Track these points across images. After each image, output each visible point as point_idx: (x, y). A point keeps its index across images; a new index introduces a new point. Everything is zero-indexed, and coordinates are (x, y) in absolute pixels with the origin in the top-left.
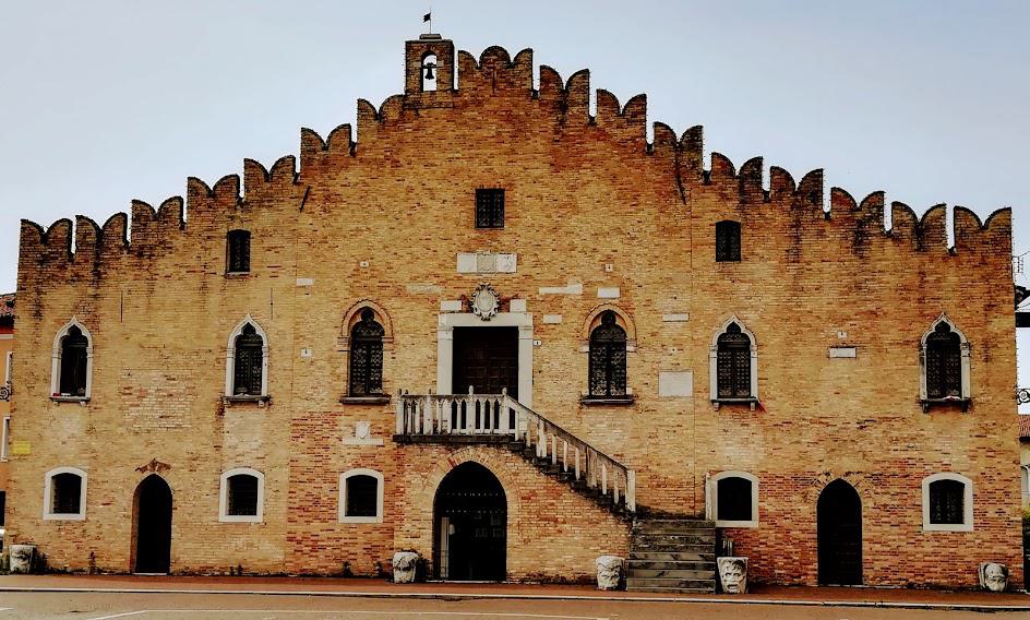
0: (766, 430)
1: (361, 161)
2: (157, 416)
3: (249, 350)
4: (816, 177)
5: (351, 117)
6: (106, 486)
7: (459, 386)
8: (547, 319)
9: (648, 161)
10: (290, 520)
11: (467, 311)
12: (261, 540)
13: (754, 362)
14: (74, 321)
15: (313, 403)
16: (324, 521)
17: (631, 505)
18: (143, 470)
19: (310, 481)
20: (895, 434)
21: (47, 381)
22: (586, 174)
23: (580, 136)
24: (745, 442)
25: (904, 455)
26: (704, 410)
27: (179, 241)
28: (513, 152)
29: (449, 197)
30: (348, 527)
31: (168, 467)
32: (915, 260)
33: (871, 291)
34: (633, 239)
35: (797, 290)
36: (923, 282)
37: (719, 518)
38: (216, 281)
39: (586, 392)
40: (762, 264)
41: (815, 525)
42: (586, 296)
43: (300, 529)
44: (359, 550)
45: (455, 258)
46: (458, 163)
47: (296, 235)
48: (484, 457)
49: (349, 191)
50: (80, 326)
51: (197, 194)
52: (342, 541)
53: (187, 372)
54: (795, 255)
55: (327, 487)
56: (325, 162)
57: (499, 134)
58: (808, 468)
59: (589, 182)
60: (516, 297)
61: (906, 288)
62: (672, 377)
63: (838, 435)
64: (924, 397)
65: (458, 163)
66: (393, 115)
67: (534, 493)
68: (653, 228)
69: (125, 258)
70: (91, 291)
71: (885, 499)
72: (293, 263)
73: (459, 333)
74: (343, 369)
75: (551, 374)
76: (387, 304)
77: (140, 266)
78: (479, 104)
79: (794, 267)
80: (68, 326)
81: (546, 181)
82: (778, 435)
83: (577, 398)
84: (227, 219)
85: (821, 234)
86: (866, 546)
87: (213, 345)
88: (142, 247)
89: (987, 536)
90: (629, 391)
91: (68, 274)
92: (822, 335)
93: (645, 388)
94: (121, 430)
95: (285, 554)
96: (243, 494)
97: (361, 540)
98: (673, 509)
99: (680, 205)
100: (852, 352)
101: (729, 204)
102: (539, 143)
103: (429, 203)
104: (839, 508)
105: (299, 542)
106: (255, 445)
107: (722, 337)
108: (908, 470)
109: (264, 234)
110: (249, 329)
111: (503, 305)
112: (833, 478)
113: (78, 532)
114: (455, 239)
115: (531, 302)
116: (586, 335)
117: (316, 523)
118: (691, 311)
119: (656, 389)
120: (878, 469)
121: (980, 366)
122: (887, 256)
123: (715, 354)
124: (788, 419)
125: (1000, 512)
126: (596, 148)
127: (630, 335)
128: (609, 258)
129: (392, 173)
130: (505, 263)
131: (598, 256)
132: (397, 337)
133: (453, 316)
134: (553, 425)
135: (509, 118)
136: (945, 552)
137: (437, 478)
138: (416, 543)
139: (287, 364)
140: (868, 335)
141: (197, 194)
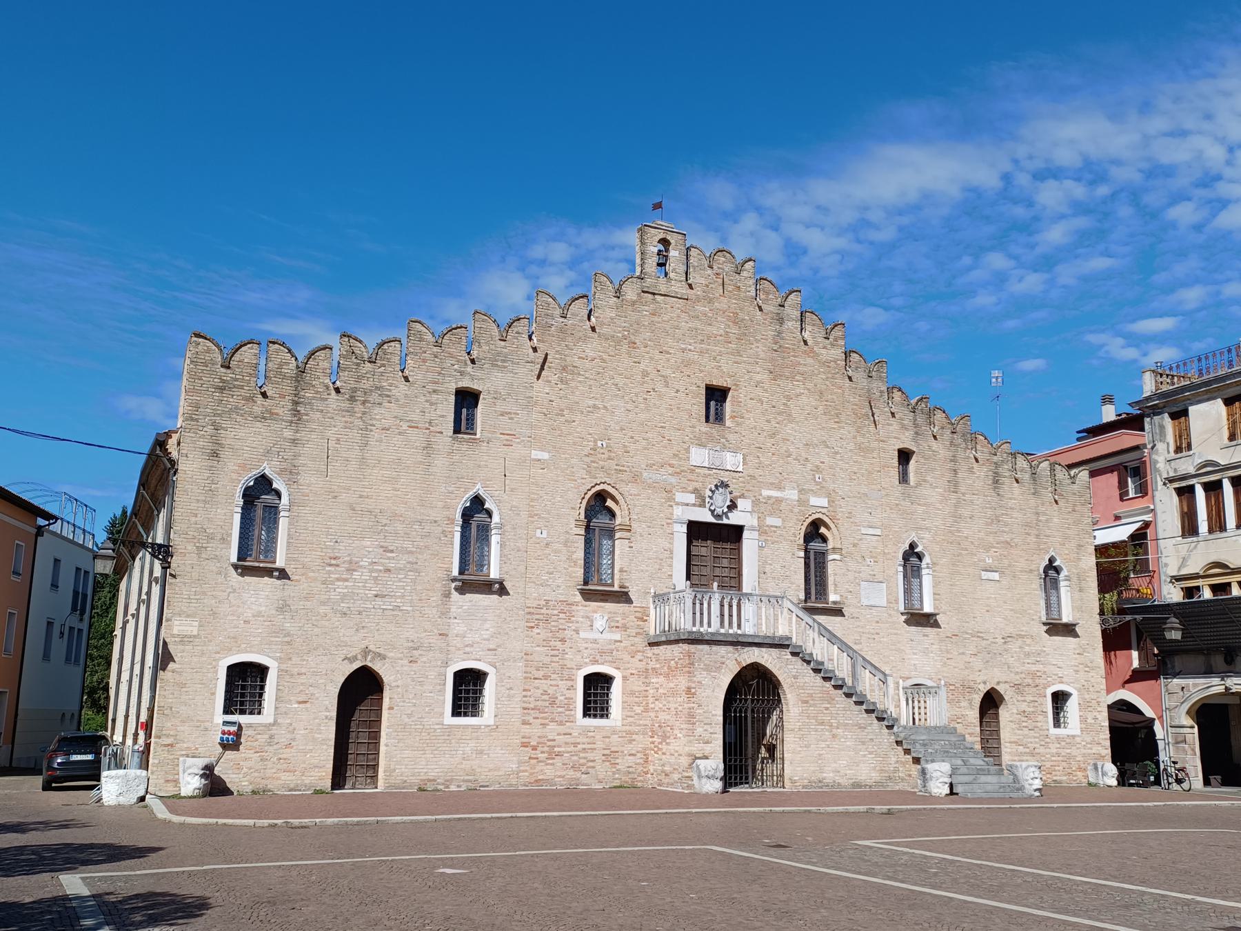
0: (941, 641)
6: (303, 679)
8: (770, 521)
10: (525, 723)
11: (700, 506)
15: (548, 590)
16: (561, 723)
18: (352, 660)
19: (546, 677)
21: (225, 540)
24: (926, 652)
25: (1034, 668)
28: (739, 354)
30: (586, 731)
31: (383, 657)
32: (1033, 501)
33: (1006, 525)
34: (836, 453)
35: (957, 517)
43: (534, 731)
44: (597, 755)
45: (688, 450)
46: (690, 355)
47: (530, 403)
48: (767, 658)
49: (588, 364)
52: (580, 747)
54: (954, 486)
55: (563, 684)
58: (971, 678)
60: (742, 496)
61: (1027, 525)
68: (851, 446)
70: (288, 434)
71: (1024, 706)
72: (528, 432)
76: (624, 488)
77: (351, 412)
78: (711, 301)
79: (953, 496)
85: (971, 470)
88: (354, 390)
89: (1089, 739)
94: (322, 609)
95: (520, 762)
97: (599, 745)
100: (996, 576)
105: (534, 748)
106: (486, 634)
108: (1037, 681)
109: (497, 397)
111: (733, 506)
112: (988, 687)
114: (688, 430)
115: (756, 503)
117: (552, 726)
120: (1016, 679)
121: (1077, 595)
130: (732, 460)
131: (809, 466)
136: (1064, 752)
140: (1006, 562)
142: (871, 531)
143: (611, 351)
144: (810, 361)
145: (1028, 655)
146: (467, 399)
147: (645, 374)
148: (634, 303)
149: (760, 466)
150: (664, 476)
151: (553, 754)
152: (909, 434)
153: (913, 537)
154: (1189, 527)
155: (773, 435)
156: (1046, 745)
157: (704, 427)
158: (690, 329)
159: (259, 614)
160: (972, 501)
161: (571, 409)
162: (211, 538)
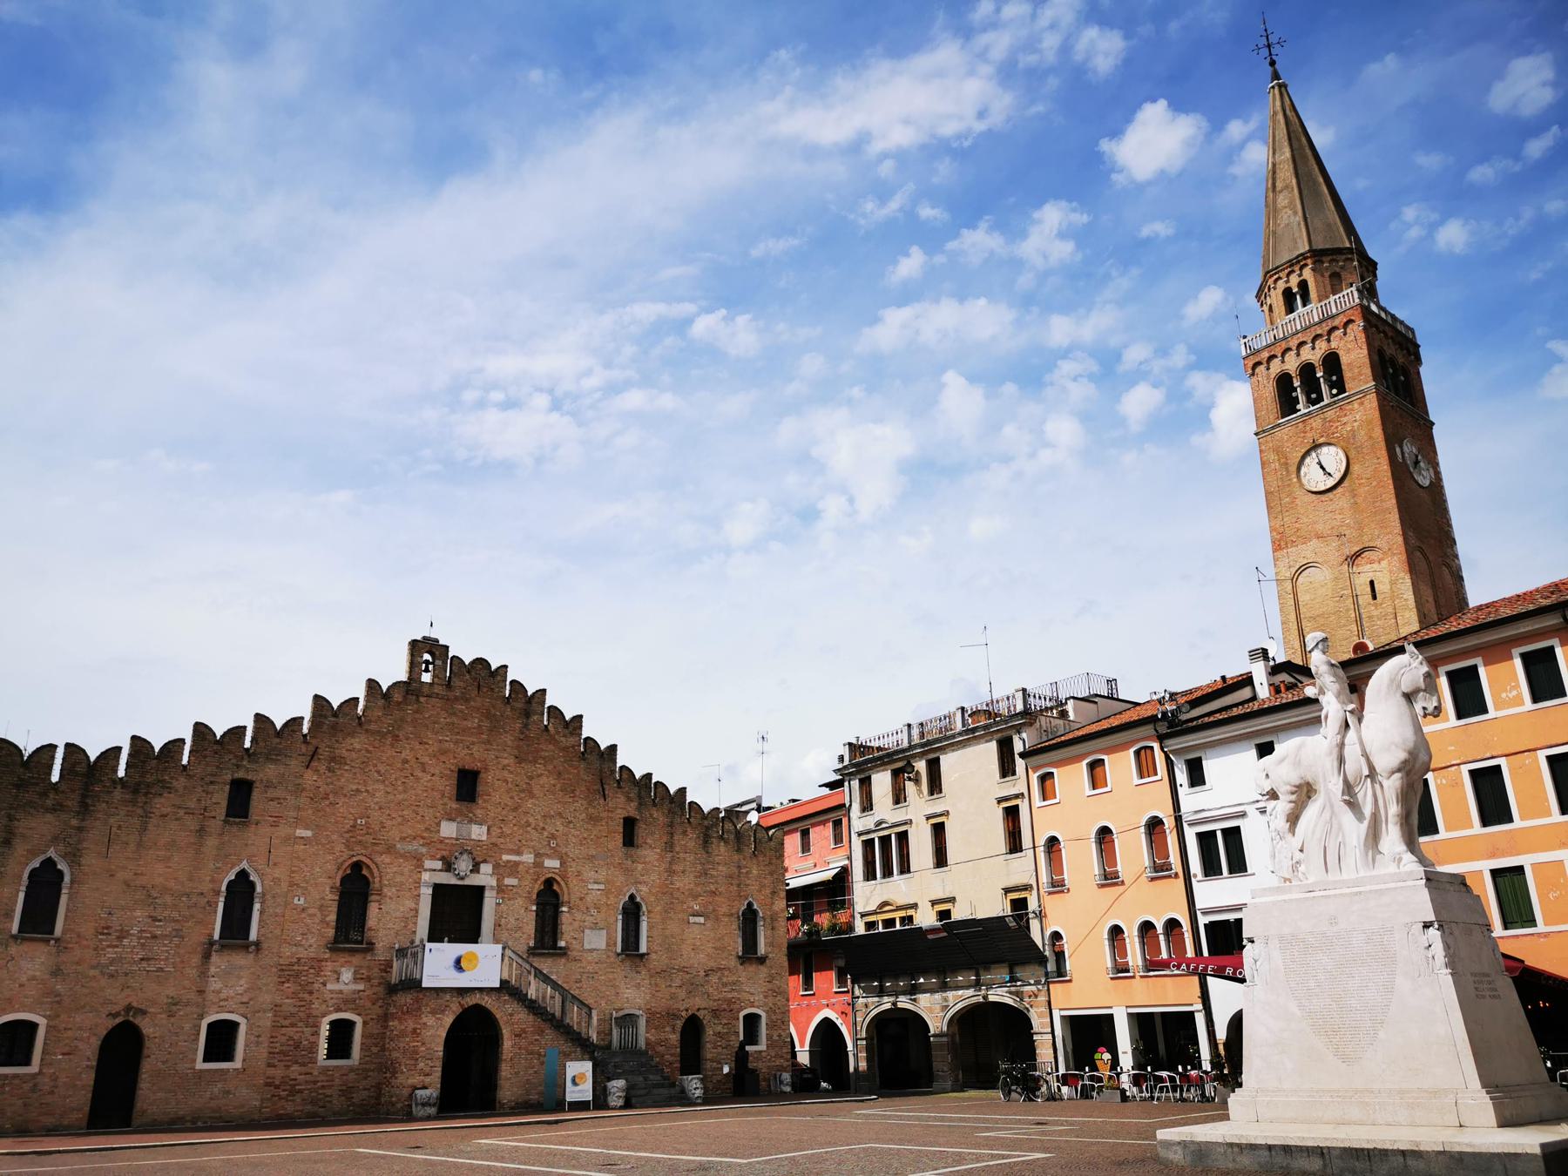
2: (137, 958)
5: (361, 693)
6: (69, 1033)
8: (508, 881)
10: (269, 1065)
14: (51, 853)
16: (303, 1065)
19: (293, 1025)
21: (9, 915)
22: (540, 768)
24: (638, 986)
27: (180, 783)
28: (489, 742)
30: (326, 1070)
31: (144, 1012)
35: (671, 872)
38: (216, 825)
40: (650, 853)
43: (278, 1073)
45: (438, 824)
47: (299, 790)
53: (175, 915)
54: (670, 846)
55: (308, 1030)
56: (334, 727)
60: (485, 861)
62: (591, 936)
66: (397, 697)
67: (524, 1031)
69: (118, 793)
70: (74, 822)
71: (719, 1028)
72: (293, 814)
73: (438, 889)
74: (333, 917)
76: (378, 859)
77: (134, 802)
78: (467, 700)
79: (669, 855)
80: (42, 858)
87: (206, 887)
88: (138, 784)
90: (562, 944)
91: (49, 802)
94: (92, 973)
100: (702, 920)
102: (508, 739)
103: (420, 775)
106: (240, 990)
109: (269, 785)
110: (243, 875)
111: (476, 869)
113: (26, 1087)
115: (496, 866)
117: (295, 1068)
118: (607, 882)
122: (721, 851)
126: (548, 749)
127: (566, 898)
128: (553, 837)
129: (392, 745)
130: (478, 832)
133: (432, 874)
135: (488, 715)
137: (449, 1020)
143: (377, 744)
144: (551, 747)
145: (725, 985)
147: (405, 761)
148: (399, 703)
151: (293, 1092)
152: (634, 804)
153: (633, 891)
154: (870, 875)
157: (455, 805)
159: (34, 978)
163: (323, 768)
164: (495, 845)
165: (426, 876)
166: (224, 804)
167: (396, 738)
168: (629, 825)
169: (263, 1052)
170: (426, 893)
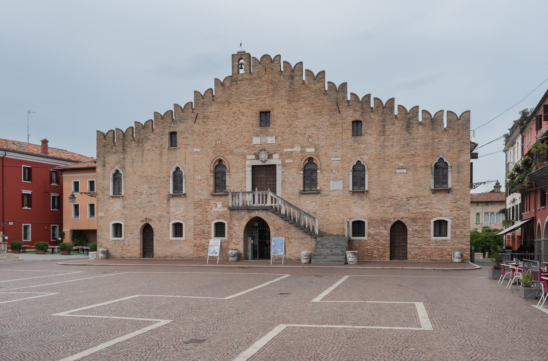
0: (371, 202)
1: (216, 102)
2: (147, 201)
3: (178, 177)
4: (392, 101)
7: (253, 189)
8: (287, 161)
9: (326, 97)
10: (195, 239)
12: (184, 246)
13: (366, 176)
14: (117, 168)
16: (206, 239)
17: (317, 232)
18: (143, 221)
19: (201, 224)
20: (421, 202)
21: (108, 190)
22: (301, 104)
23: (299, 89)
24: (363, 207)
25: (424, 211)
26: (347, 194)
27: (152, 136)
28: (273, 96)
29: (249, 115)
31: (151, 220)
32: (431, 133)
33: (412, 146)
35: (383, 147)
36: (433, 142)
37: (353, 236)
38: (166, 151)
39: (302, 189)
41: (389, 238)
42: (302, 152)
43: (198, 242)
45: (252, 139)
46: (253, 102)
47: (193, 132)
48: (262, 215)
49: (213, 114)
50: (119, 169)
51: (157, 118)
53: (156, 186)
54: (383, 132)
55: (207, 226)
56: (203, 104)
57: (268, 89)
58: (387, 216)
59: (302, 107)
60: (275, 153)
62: (335, 183)
63: (398, 203)
64: (433, 188)
65: (253, 102)
67: (280, 228)
68: (327, 124)
69: (133, 144)
70: (122, 156)
71: (417, 228)
72: (193, 143)
73: (254, 167)
74: (212, 182)
75: (289, 182)
76: (227, 157)
77: (138, 146)
79: (382, 138)
81: (286, 107)
82: (375, 204)
83: (298, 191)
84: (169, 128)
85: (393, 124)
86: (409, 246)
87: (165, 175)
88: (139, 139)
90: (318, 188)
91: (114, 150)
92: (393, 164)
93: (324, 187)
94: (134, 207)
95: (193, 251)
96: (178, 229)
98: (335, 233)
99: (338, 115)
100: (405, 171)
101: (357, 113)
102: (283, 92)
103: (242, 118)
104: (398, 230)
106: (181, 212)
107: (354, 166)
108: (426, 216)
109: (182, 132)
110: (178, 168)
111: (270, 156)
112: (396, 220)
113: (122, 244)
115: (281, 155)
116: (302, 167)
117: (204, 240)
119: (329, 187)
121: (455, 175)
123: (351, 173)
124: (379, 198)
125: (462, 232)
126: (305, 93)
127: (319, 166)
128: (310, 137)
129: (228, 107)
130: (271, 140)
131: (306, 136)
132: (231, 170)
133: (251, 161)
134: (287, 202)
135: (272, 82)
137: (244, 223)
138: (237, 247)
139: (191, 181)
140: (411, 164)
141: (157, 118)
142: (336, 159)
144: (307, 91)
146: (173, 134)
147: (235, 113)
148: (229, 87)
149: (283, 140)
150: (243, 150)
155: (290, 126)
156: (428, 244)
157: (259, 129)
158: (252, 91)
159: (118, 210)
160: (393, 139)
161: (207, 132)
162: (105, 189)
163: (201, 122)
164: (279, 145)
165: (248, 163)
166: (167, 142)
167: (229, 103)
168: (357, 123)
169: (191, 234)
170: (249, 170)
